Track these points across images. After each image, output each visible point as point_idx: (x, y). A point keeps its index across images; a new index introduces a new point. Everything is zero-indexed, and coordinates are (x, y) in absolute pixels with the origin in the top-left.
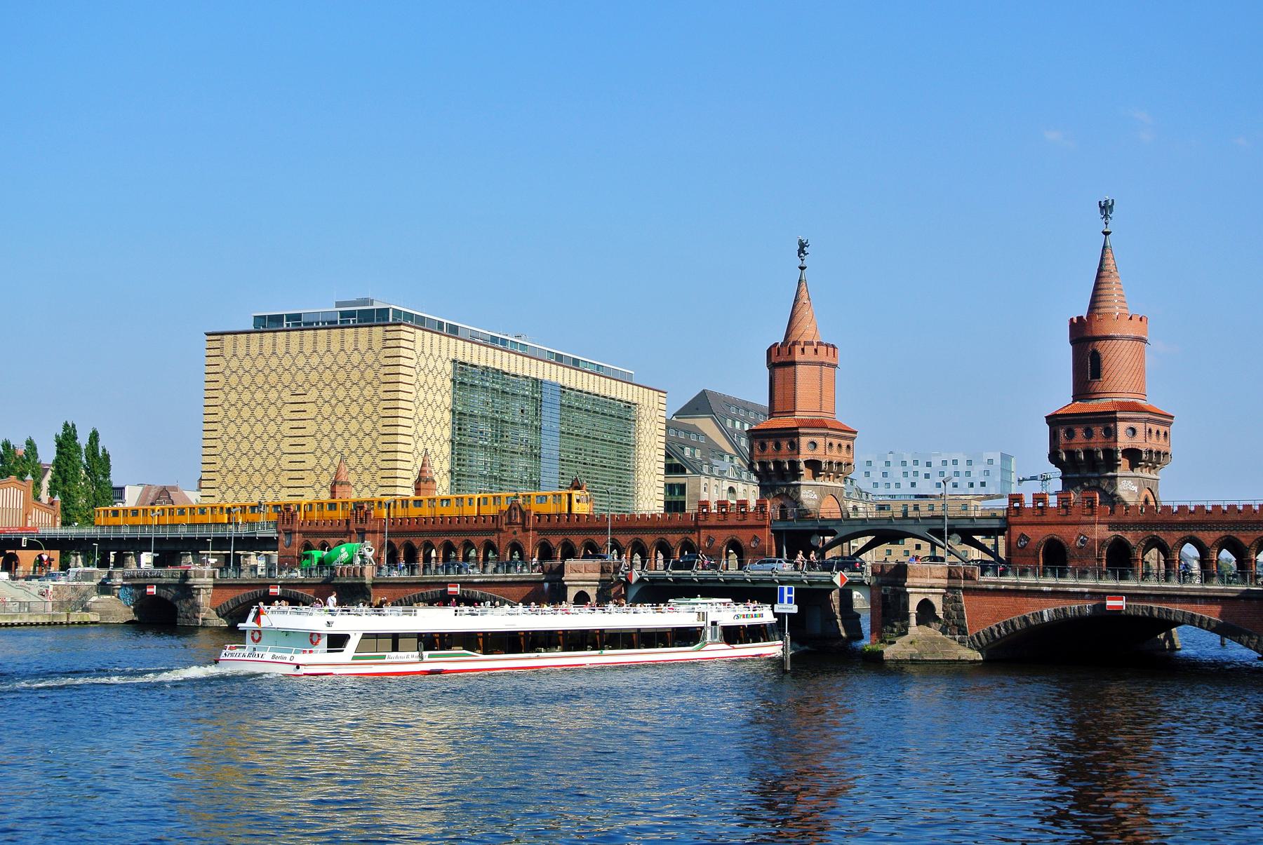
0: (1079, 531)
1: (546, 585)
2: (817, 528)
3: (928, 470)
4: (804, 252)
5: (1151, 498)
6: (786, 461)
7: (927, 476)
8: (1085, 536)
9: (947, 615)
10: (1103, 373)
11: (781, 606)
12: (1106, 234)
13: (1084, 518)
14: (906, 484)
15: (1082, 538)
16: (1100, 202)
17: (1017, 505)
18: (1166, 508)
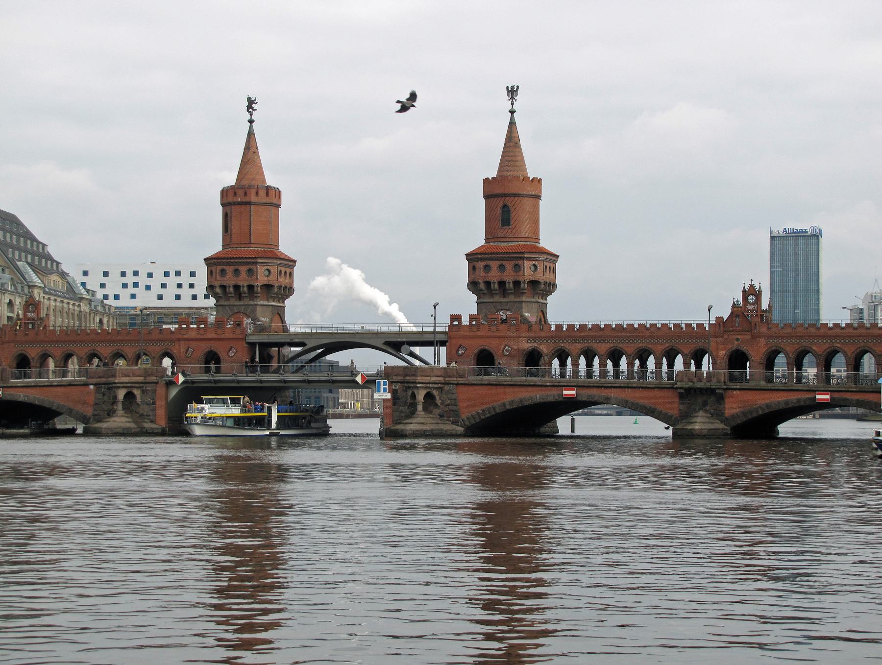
0: (504, 343)
1: (92, 387)
2: (289, 341)
3: (149, 281)
4: (252, 108)
5: (543, 319)
6: (245, 285)
7: (148, 287)
8: (509, 347)
9: (442, 404)
10: (512, 222)
11: (379, 394)
12: (512, 112)
13: (509, 333)
14: (125, 294)
15: (507, 348)
16: (507, 87)
17: (456, 323)
18: (559, 327)
